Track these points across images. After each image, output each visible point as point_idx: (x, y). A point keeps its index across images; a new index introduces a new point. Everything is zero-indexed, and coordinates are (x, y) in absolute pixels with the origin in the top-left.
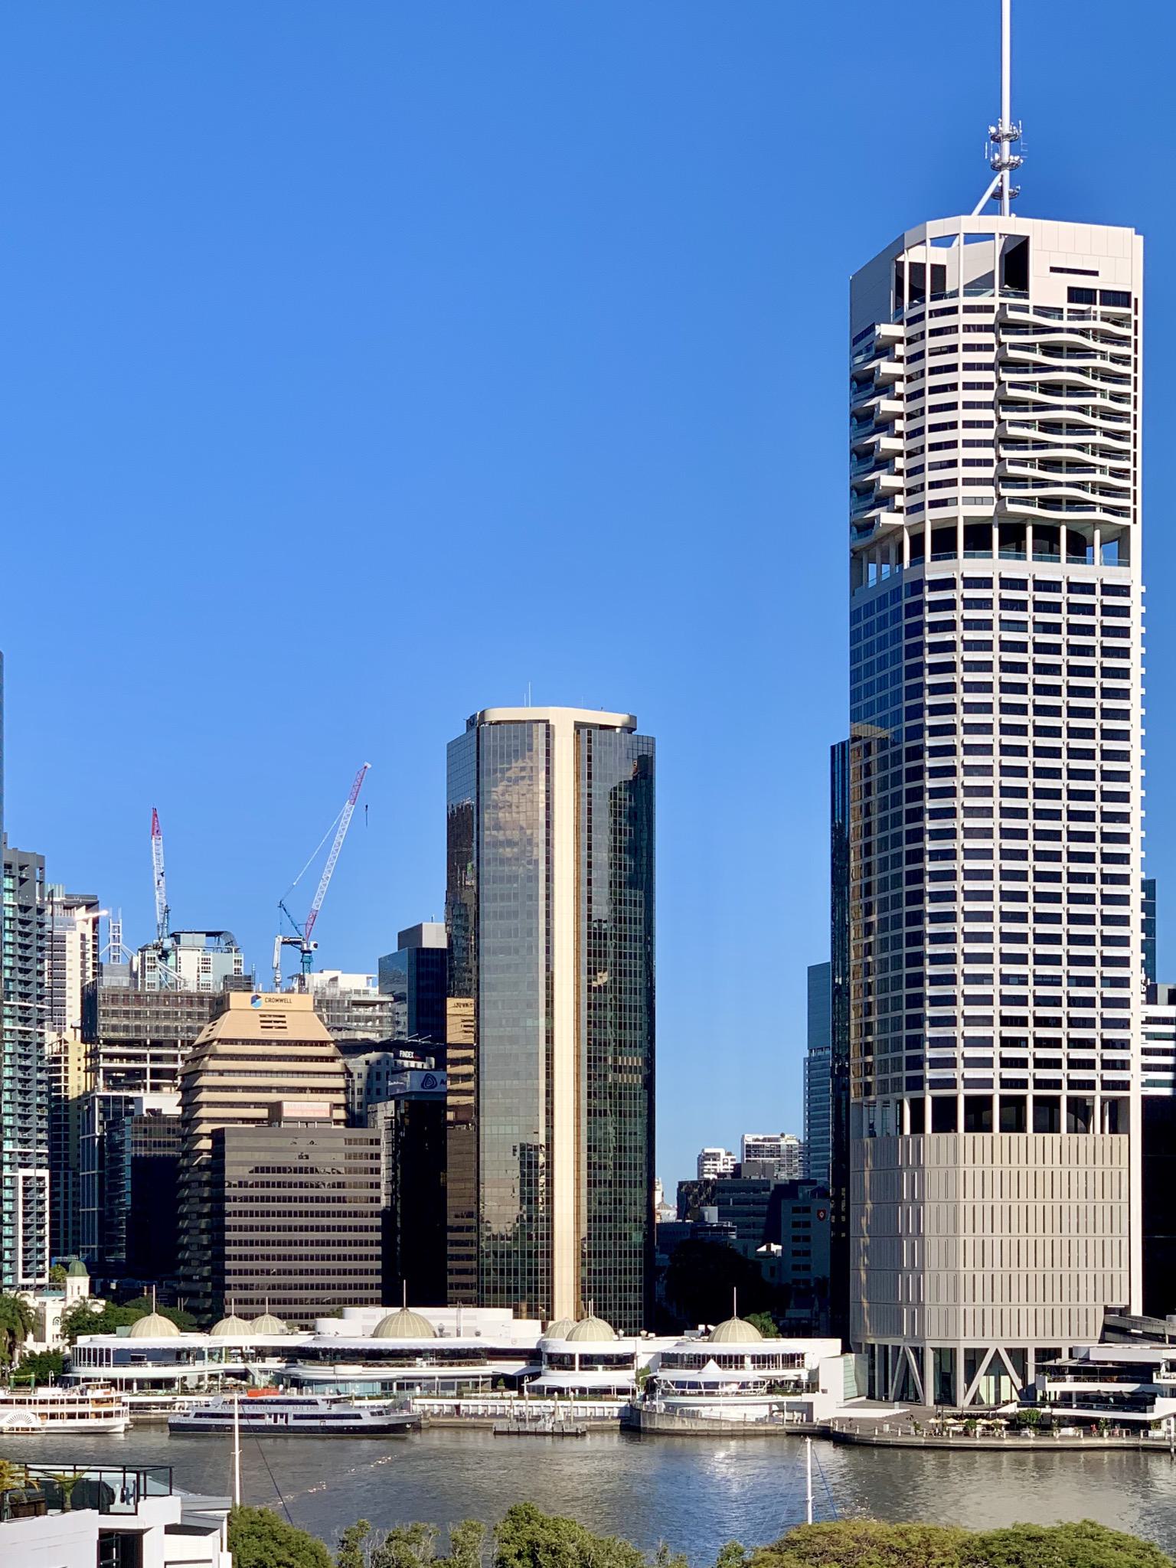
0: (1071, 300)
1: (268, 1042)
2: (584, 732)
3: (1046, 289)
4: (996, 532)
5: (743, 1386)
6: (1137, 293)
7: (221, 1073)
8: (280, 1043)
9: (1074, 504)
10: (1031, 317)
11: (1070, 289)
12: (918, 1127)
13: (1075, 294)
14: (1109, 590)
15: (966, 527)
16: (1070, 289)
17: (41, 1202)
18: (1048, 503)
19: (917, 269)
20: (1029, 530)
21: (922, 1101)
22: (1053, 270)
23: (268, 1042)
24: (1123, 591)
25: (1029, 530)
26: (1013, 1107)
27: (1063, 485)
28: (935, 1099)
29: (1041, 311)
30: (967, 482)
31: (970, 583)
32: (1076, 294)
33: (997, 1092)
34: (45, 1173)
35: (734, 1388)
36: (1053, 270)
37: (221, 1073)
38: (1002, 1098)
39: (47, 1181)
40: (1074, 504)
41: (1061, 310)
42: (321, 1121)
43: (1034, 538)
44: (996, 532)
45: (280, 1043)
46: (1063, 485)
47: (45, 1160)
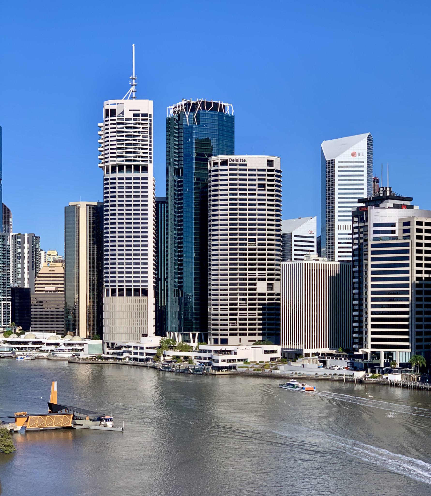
0: (134, 116)
1: (50, 274)
2: (88, 207)
3: (129, 115)
4: (117, 168)
5: (69, 350)
6: (150, 111)
7: (40, 280)
8: (53, 274)
9: (135, 161)
10: (125, 122)
11: (134, 114)
12: (108, 295)
13: (135, 115)
14: (143, 178)
15: (111, 167)
16: (134, 114)
17: (9, 309)
18: (127, 161)
19: (107, 110)
20: (125, 167)
21: (109, 289)
22: (130, 110)
23: (50, 274)
24: (147, 178)
25: (125, 167)
26: (121, 290)
27: (131, 157)
28: (112, 289)
29: (127, 120)
30: (111, 157)
31: (119, 179)
32: (135, 115)
33: (117, 288)
34: (10, 302)
35: (67, 350)
36: (130, 110)
37: (40, 280)
38: (118, 289)
39: (11, 304)
40: (135, 161)
41: (131, 119)
42: (53, 291)
43: (126, 168)
44: (117, 168)
45: (53, 274)
46: (131, 157)
47: (10, 300)
